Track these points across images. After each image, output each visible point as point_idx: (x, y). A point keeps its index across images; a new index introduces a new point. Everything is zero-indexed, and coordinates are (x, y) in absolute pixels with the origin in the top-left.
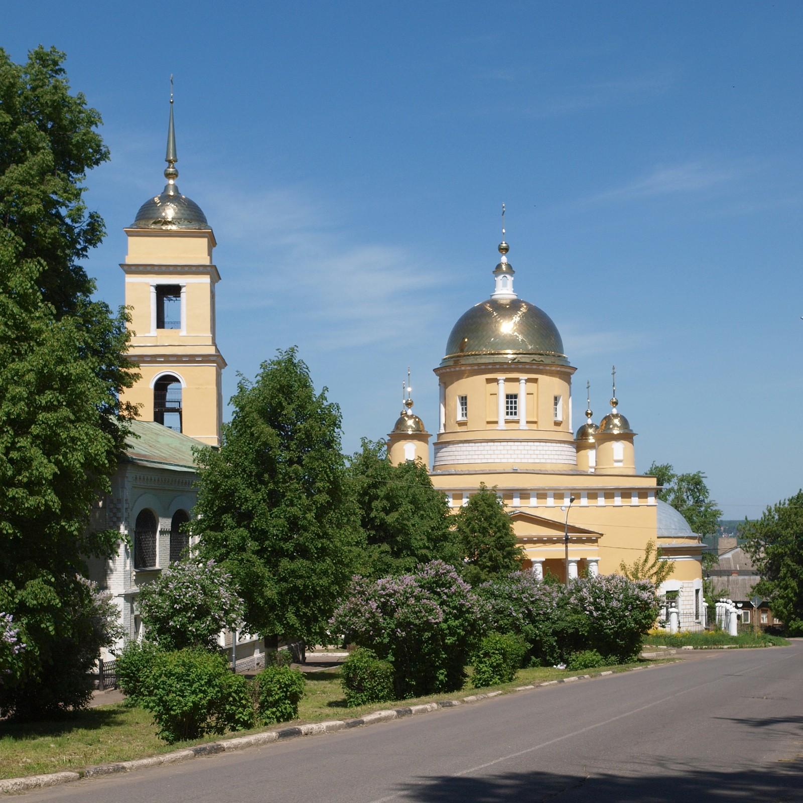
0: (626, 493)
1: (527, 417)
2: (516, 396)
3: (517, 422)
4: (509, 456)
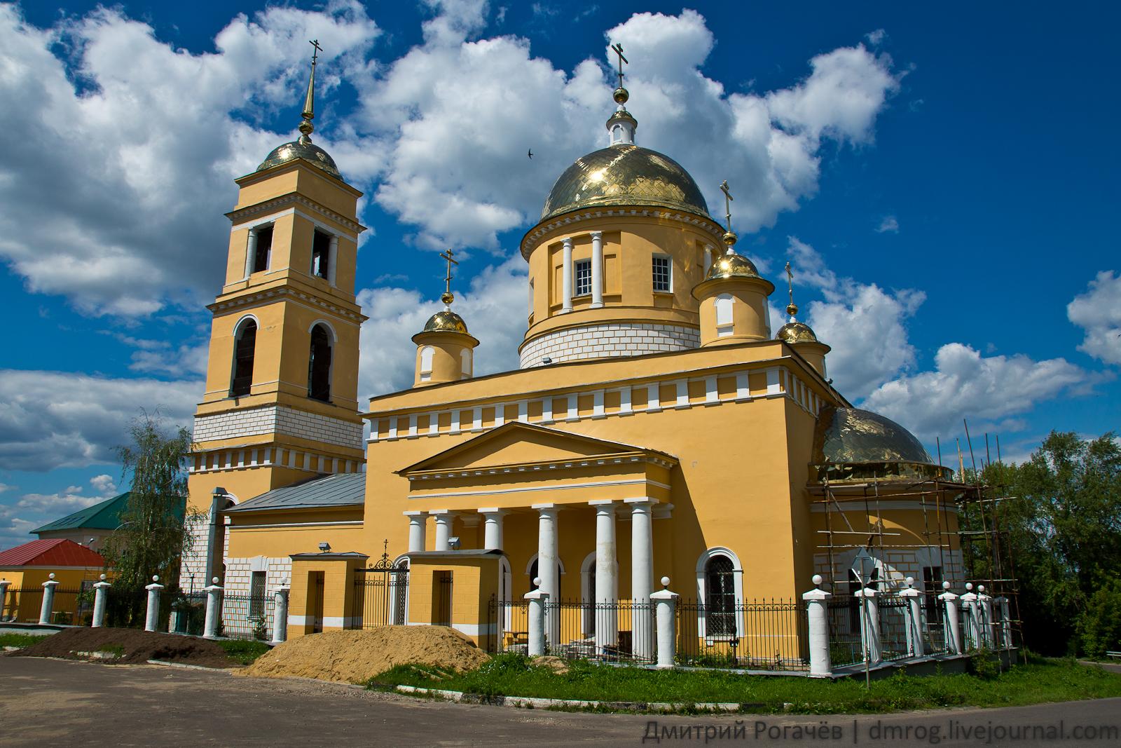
0: (726, 378)
1: (604, 289)
2: (590, 263)
3: (589, 300)
4: (570, 352)
